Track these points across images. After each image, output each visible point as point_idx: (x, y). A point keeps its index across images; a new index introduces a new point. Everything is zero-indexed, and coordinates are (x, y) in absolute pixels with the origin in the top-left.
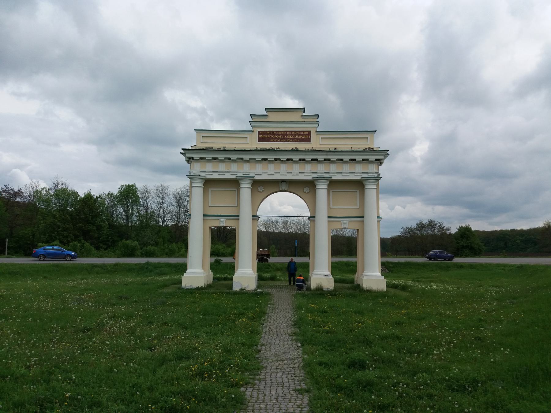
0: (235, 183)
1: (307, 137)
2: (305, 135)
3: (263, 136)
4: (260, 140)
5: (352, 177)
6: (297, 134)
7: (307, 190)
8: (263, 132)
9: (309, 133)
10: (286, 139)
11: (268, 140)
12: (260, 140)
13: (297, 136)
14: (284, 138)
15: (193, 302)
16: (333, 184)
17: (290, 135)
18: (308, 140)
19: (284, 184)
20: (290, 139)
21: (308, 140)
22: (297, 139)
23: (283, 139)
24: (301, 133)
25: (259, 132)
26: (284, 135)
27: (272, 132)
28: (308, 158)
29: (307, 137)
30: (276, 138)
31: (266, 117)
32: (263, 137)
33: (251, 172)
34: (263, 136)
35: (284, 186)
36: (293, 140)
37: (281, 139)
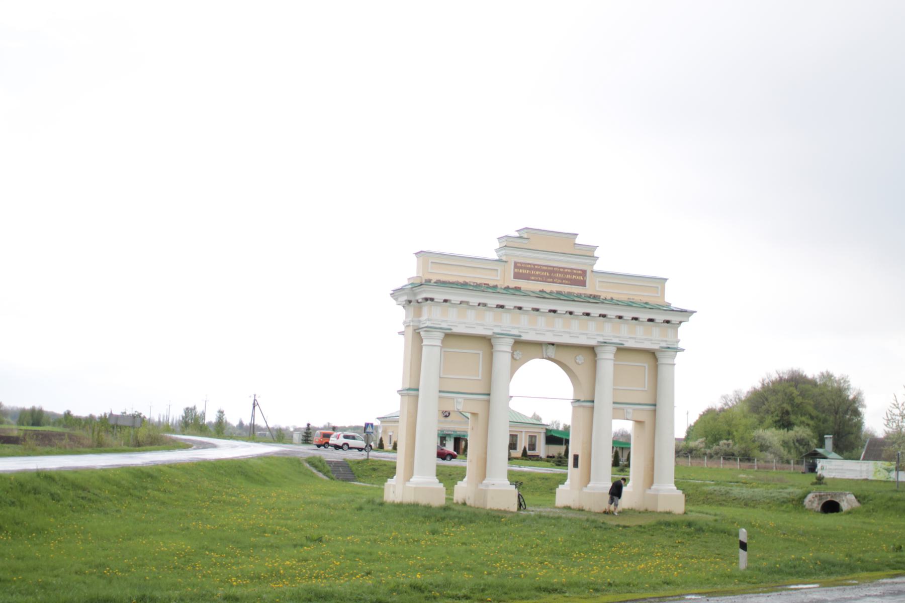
0: (487, 341)
1: (581, 278)
2: (579, 275)
3: (521, 271)
4: (517, 276)
5: (647, 345)
6: (567, 273)
7: (581, 358)
8: (522, 263)
9: (584, 272)
10: (555, 278)
11: (527, 277)
12: (517, 276)
13: (568, 276)
14: (550, 277)
15: (272, 546)
16: (622, 350)
17: (560, 272)
18: (583, 284)
19: (551, 347)
20: (559, 278)
21: (583, 284)
22: (568, 279)
23: (548, 277)
24: (572, 271)
25: (516, 264)
26: (550, 272)
27: (535, 265)
28: (644, 316)
29: (581, 278)
30: (539, 276)
31: (526, 241)
32: (523, 271)
33: (513, 328)
34: (521, 271)
35: (551, 351)
36: (562, 281)
37: (547, 277)
